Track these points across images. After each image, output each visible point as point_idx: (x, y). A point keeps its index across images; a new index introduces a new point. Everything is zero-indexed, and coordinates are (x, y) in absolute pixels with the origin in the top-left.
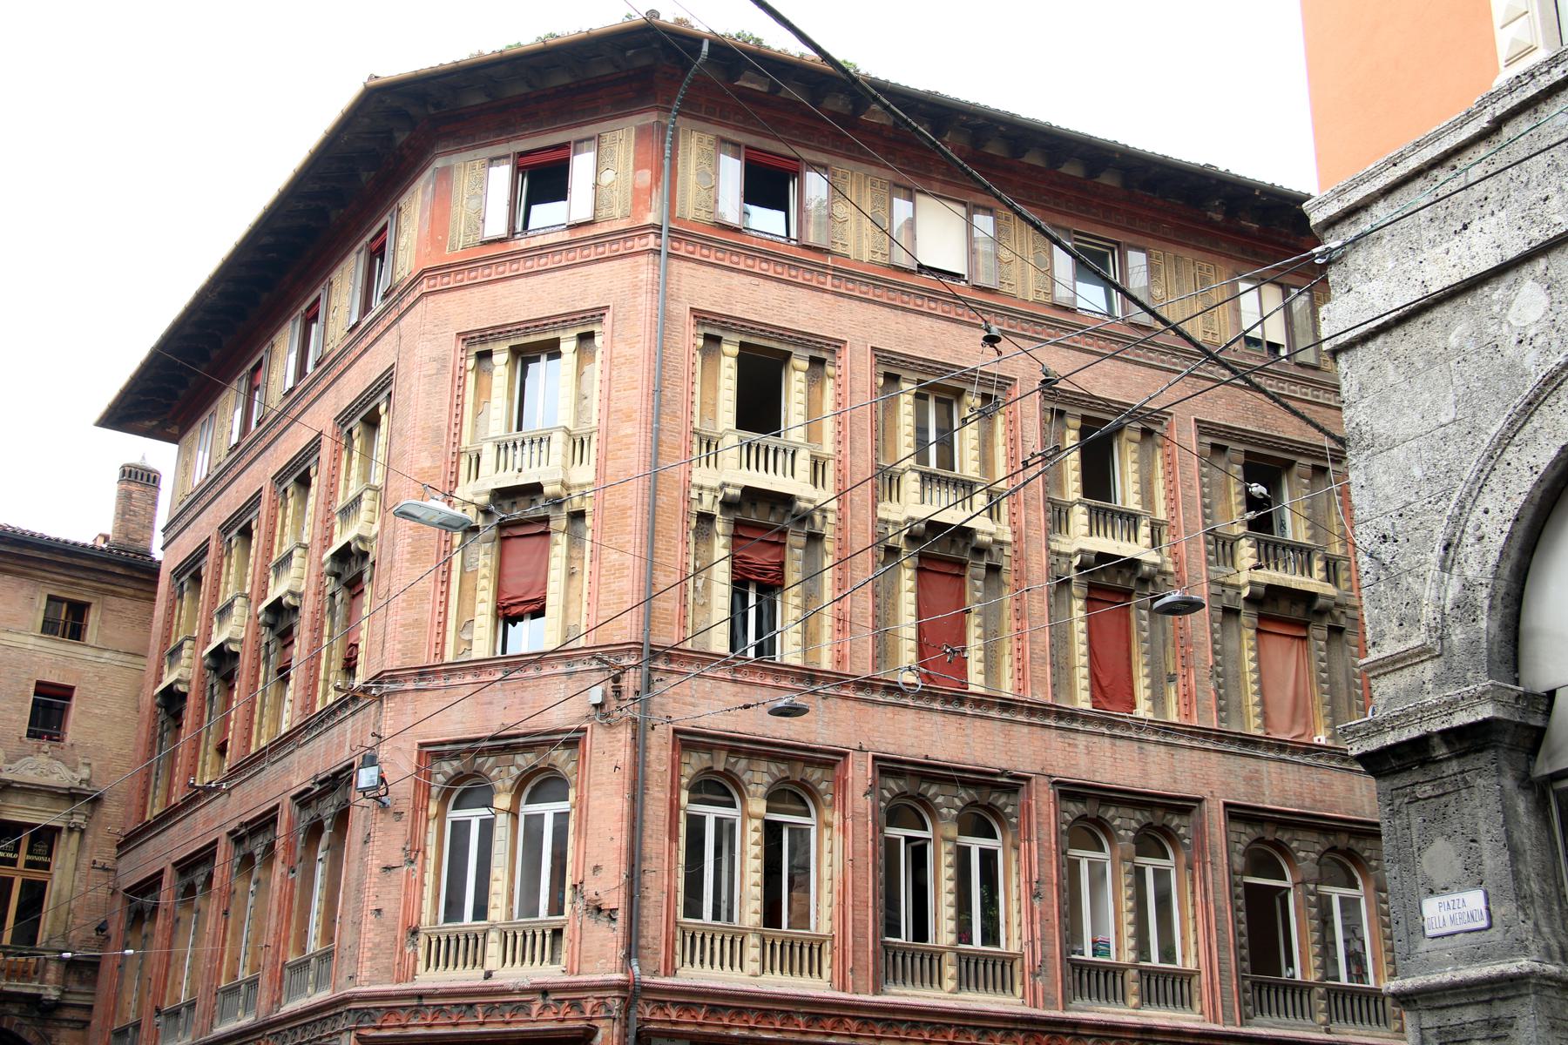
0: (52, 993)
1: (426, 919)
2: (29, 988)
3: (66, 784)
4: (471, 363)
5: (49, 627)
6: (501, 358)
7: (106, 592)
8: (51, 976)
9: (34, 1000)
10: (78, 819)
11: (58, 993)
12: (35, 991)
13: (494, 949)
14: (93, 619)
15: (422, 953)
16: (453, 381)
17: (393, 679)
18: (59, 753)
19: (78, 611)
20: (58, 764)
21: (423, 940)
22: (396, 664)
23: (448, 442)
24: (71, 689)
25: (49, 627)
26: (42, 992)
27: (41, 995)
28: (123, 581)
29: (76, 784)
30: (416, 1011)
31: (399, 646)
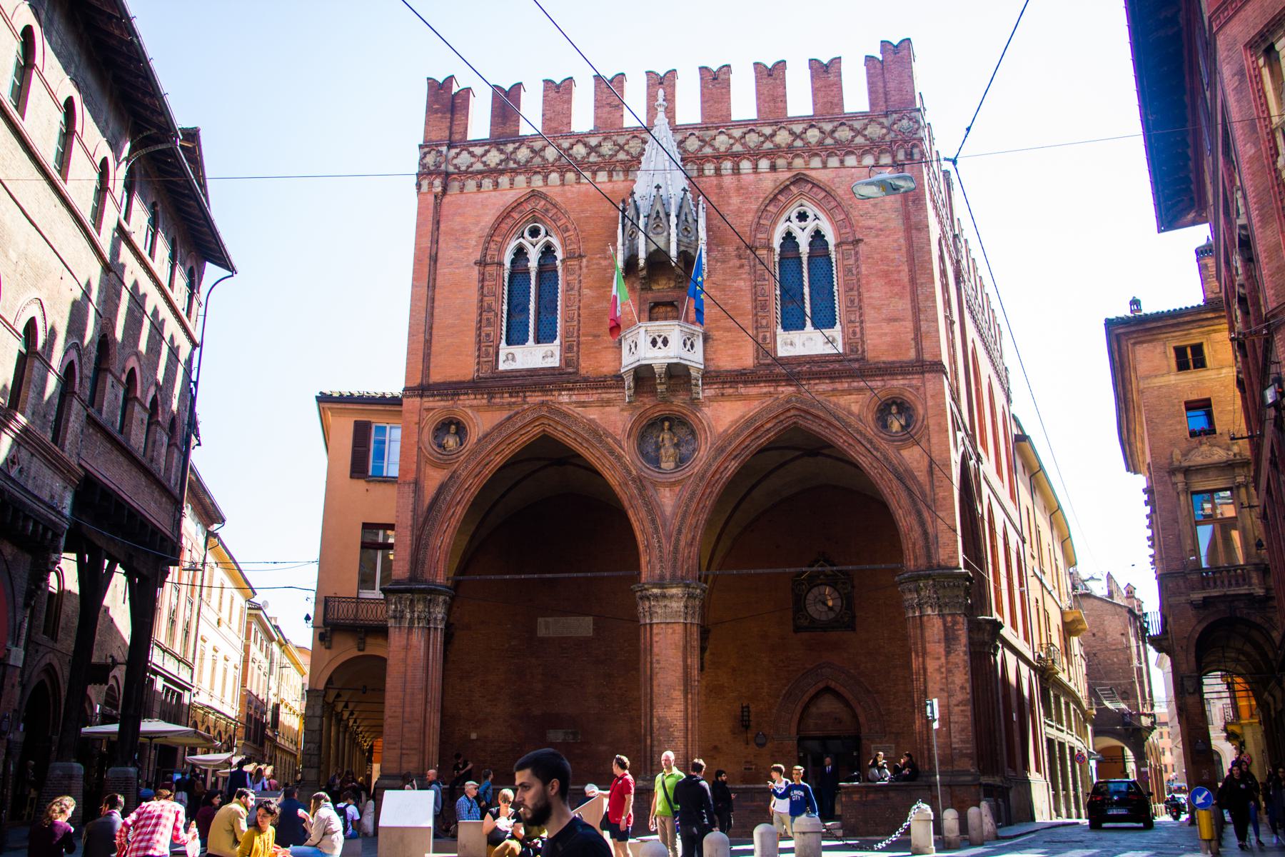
0: (1260, 591)
2: (1243, 590)
3: (1225, 459)
4: (1261, 62)
5: (1182, 366)
7: (1209, 333)
8: (1255, 580)
9: (1250, 596)
10: (1240, 479)
11: (1263, 591)
12: (1247, 592)
14: (1207, 351)
16: (1251, 81)
17: (1274, 316)
18: (1214, 442)
19: (1198, 349)
20: (1215, 448)
22: (1275, 305)
23: (1261, 127)
24: (1209, 400)
25: (1182, 366)
26: (1252, 591)
27: (1252, 594)
28: (1217, 321)
29: (1232, 457)
31: (1272, 292)
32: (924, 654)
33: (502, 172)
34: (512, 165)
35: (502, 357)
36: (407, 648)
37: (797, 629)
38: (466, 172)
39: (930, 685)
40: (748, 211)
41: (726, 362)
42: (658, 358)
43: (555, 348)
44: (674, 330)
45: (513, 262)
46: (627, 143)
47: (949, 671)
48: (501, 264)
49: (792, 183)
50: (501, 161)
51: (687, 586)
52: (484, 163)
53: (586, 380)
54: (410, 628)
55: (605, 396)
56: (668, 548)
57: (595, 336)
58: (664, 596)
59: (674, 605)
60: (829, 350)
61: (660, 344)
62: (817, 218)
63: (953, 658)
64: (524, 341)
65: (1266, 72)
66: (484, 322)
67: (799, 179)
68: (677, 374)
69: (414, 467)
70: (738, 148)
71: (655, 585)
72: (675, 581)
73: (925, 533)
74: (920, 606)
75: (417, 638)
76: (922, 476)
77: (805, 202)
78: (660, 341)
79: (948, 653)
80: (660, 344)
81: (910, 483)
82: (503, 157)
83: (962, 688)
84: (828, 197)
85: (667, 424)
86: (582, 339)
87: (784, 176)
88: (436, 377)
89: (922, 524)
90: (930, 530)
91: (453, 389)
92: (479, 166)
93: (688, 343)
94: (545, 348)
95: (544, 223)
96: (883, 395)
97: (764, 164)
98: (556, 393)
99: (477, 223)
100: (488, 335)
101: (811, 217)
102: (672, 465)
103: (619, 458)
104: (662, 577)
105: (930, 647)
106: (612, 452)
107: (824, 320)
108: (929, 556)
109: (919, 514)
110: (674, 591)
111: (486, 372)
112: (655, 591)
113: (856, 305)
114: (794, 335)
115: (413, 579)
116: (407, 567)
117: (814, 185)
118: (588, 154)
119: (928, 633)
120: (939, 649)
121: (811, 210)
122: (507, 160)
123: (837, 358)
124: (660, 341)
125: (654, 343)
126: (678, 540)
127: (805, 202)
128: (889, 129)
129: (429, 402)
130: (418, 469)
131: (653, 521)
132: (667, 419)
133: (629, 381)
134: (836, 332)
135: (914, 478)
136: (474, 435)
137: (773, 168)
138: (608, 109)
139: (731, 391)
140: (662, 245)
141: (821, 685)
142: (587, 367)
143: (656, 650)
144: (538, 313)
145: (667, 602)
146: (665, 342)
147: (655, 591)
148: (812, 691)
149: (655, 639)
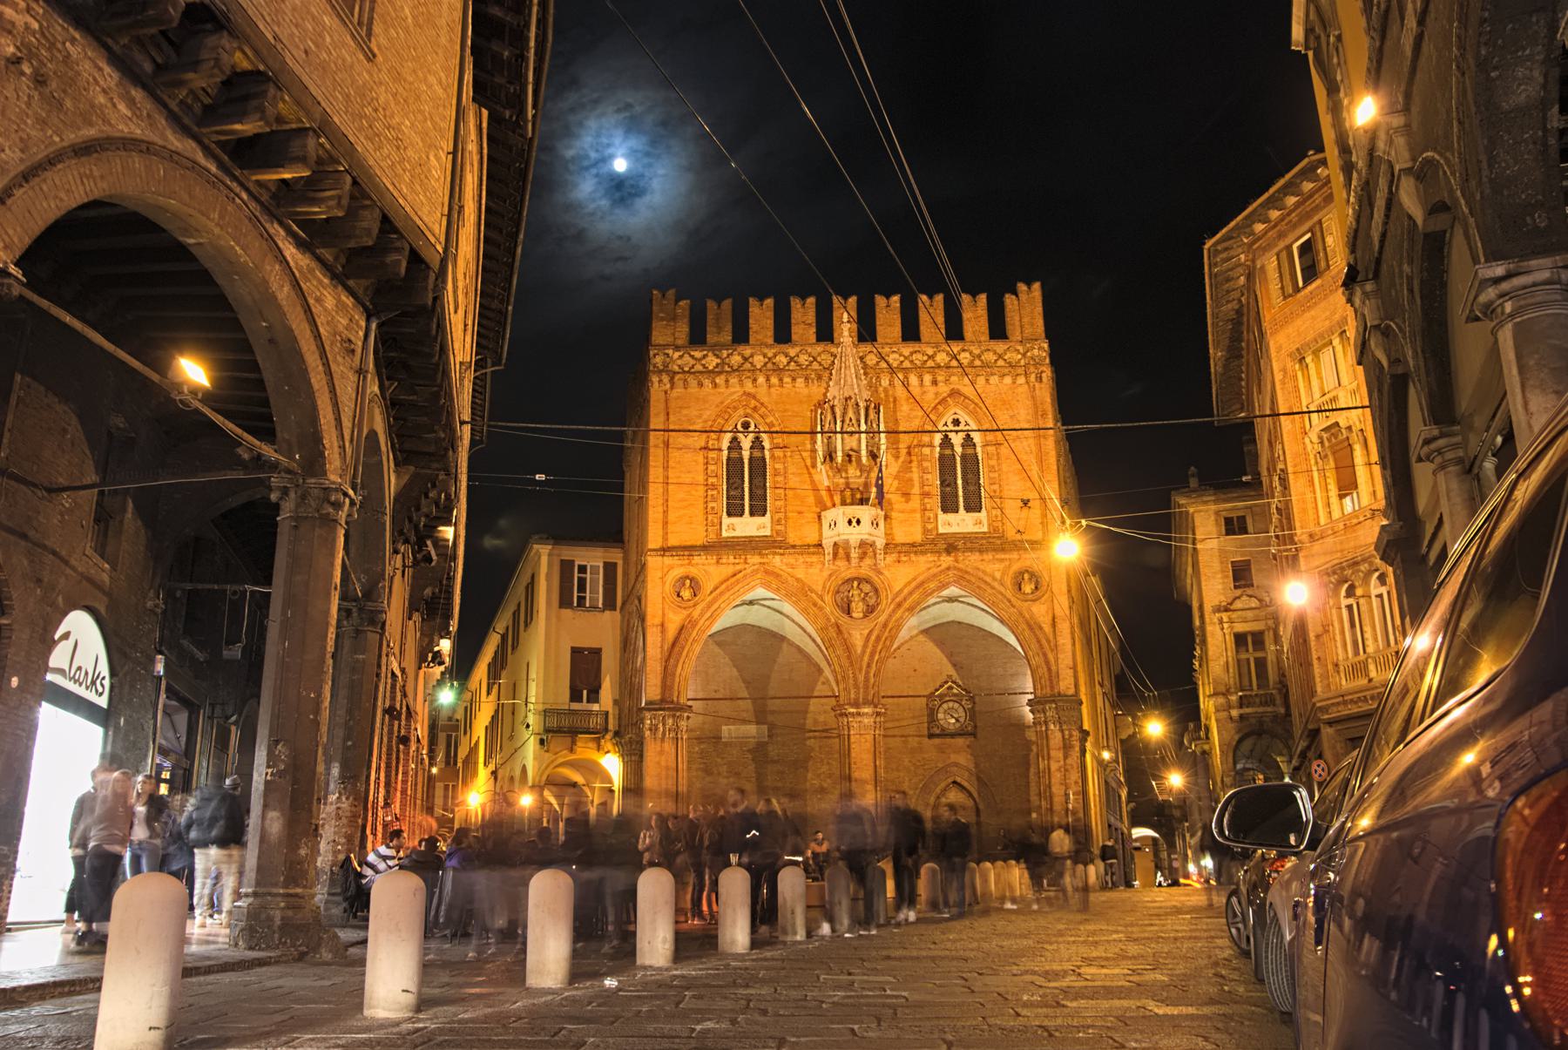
1: (1341, 658)
4: (1297, 366)
6: (1309, 360)
13: (1372, 667)
15: (1342, 675)
21: (1342, 668)
30: (1345, 703)
32: (1049, 758)
33: (720, 373)
34: (727, 368)
35: (724, 527)
36: (661, 752)
37: (931, 736)
38: (688, 372)
39: (1053, 781)
40: (916, 417)
41: (900, 537)
42: (854, 535)
43: (766, 520)
44: (866, 513)
45: (729, 448)
46: (819, 354)
47: (1066, 770)
48: (720, 450)
49: (950, 396)
50: (718, 365)
51: (876, 707)
52: (704, 366)
53: (794, 547)
54: (663, 739)
55: (809, 560)
56: (861, 678)
57: (800, 513)
58: (859, 714)
59: (866, 721)
60: (976, 529)
61: (854, 523)
62: (967, 424)
63: (1069, 761)
64: (741, 515)
65: (1299, 374)
66: (709, 498)
67: (955, 393)
68: (866, 547)
69: (660, 612)
70: (907, 364)
71: (852, 705)
72: (866, 703)
73: (1049, 669)
74: (1046, 723)
75: (668, 746)
76: (1047, 628)
77: (959, 411)
78: (854, 521)
79: (1066, 757)
80: (854, 523)
81: (1038, 632)
82: (719, 361)
83: (1076, 783)
84: (977, 406)
85: (855, 584)
86: (790, 515)
87: (944, 389)
88: (673, 542)
89: (1047, 663)
90: (1054, 668)
91: (688, 550)
92: (699, 367)
93: (875, 524)
94: (758, 520)
95: (753, 418)
96: (1016, 567)
97: (927, 378)
98: (770, 557)
99: (700, 416)
100: (713, 508)
101: (963, 423)
102: (861, 615)
103: (821, 609)
104: (857, 700)
105: (1053, 753)
106: (815, 605)
107: (973, 506)
108: (1052, 688)
109: (1045, 655)
110: (866, 710)
111: (712, 537)
112: (852, 710)
113: (996, 497)
114: (950, 517)
115: (663, 700)
116: (659, 691)
117: (966, 397)
118: (788, 363)
119: (1052, 743)
120: (1061, 755)
121: (963, 417)
122: (723, 363)
123: (983, 536)
124: (854, 521)
125: (850, 522)
126: (867, 673)
127: (959, 411)
128: (1024, 355)
129: (668, 560)
130: (664, 615)
131: (849, 657)
132: (855, 579)
133: (829, 549)
134: (983, 515)
135: (1041, 628)
136: (708, 586)
137: (935, 383)
138: (802, 326)
139: (904, 559)
140: (854, 445)
141: (950, 780)
142: (792, 538)
143: (853, 755)
144: (750, 490)
145: (859, 719)
146: (858, 522)
147: (852, 710)
148: (943, 785)
149: (853, 746)
